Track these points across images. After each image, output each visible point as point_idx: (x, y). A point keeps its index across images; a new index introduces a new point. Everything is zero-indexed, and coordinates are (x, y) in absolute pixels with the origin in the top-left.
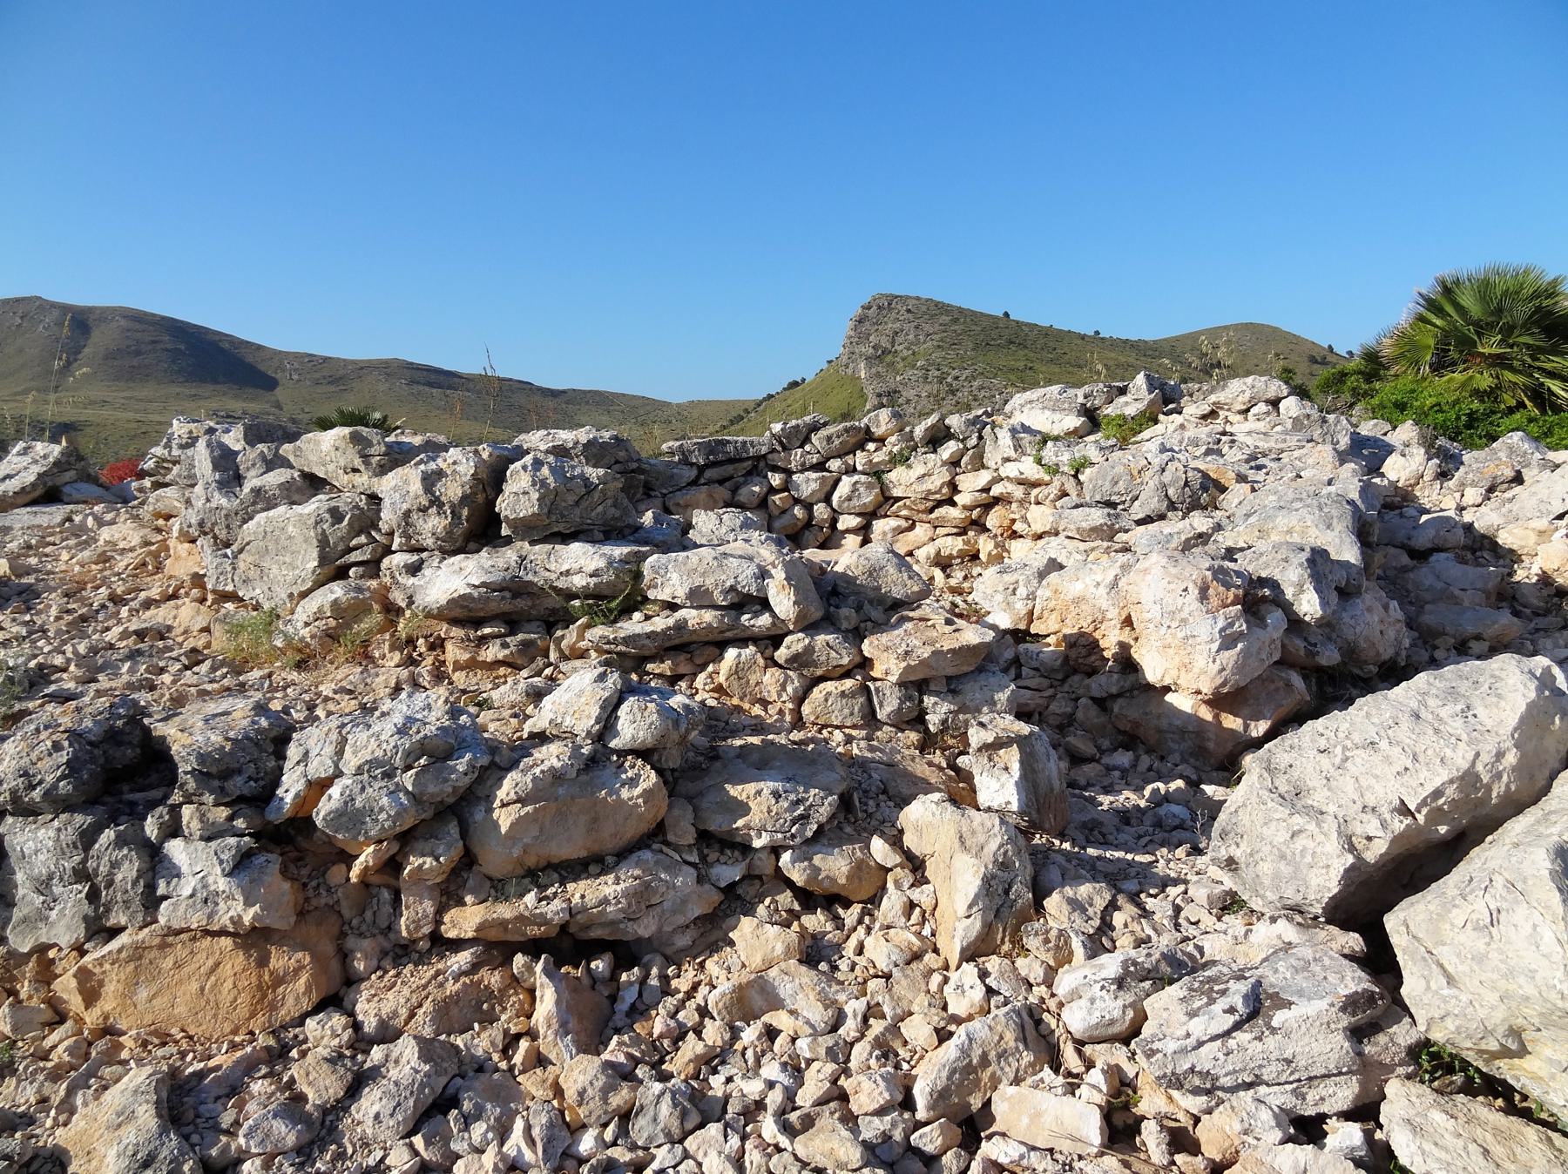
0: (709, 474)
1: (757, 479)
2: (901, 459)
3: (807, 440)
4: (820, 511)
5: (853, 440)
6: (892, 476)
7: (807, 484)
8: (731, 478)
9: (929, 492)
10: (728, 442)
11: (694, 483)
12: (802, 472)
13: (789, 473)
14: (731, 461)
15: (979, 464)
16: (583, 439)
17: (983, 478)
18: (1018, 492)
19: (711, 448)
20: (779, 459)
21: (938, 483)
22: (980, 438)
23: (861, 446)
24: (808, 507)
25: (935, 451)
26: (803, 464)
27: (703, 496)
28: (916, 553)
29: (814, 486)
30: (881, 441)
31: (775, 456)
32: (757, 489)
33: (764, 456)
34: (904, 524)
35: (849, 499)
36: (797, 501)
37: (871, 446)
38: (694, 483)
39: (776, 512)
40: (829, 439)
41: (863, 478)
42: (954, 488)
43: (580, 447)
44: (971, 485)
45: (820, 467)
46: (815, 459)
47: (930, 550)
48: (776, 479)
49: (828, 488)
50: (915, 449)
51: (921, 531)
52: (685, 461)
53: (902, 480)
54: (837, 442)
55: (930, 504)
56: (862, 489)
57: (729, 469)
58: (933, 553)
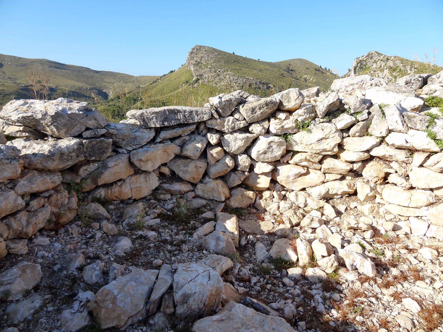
0: (164, 135)
1: (199, 138)
2: (302, 126)
3: (237, 110)
4: (243, 160)
5: (269, 111)
6: (296, 137)
7: (235, 142)
8: (180, 136)
9: (325, 150)
10: (179, 111)
12: (231, 133)
13: (222, 133)
14: (181, 125)
15: (365, 132)
16: (52, 111)
17: (368, 142)
18: (401, 155)
19: (166, 116)
20: (216, 124)
21: (332, 146)
22: (369, 113)
23: (273, 115)
24: (234, 157)
25: (330, 121)
26: (233, 128)
27: (160, 152)
28: (309, 190)
29: (240, 143)
30: (290, 112)
31: (213, 121)
32: (199, 145)
33: (205, 122)
34: (303, 171)
35: (265, 153)
36: (226, 153)
37: (282, 116)
38: (153, 141)
39: (212, 162)
40: (253, 110)
41: (276, 139)
42: (341, 146)
43: (48, 120)
44: (355, 147)
45: (245, 130)
46: (242, 124)
47: (322, 190)
48: (213, 139)
49: (249, 144)
50: (314, 119)
51: (315, 176)
52: (145, 126)
53: (301, 140)
54: (259, 113)
55: (320, 157)
56: (274, 146)
57: (179, 131)
58: (323, 192)
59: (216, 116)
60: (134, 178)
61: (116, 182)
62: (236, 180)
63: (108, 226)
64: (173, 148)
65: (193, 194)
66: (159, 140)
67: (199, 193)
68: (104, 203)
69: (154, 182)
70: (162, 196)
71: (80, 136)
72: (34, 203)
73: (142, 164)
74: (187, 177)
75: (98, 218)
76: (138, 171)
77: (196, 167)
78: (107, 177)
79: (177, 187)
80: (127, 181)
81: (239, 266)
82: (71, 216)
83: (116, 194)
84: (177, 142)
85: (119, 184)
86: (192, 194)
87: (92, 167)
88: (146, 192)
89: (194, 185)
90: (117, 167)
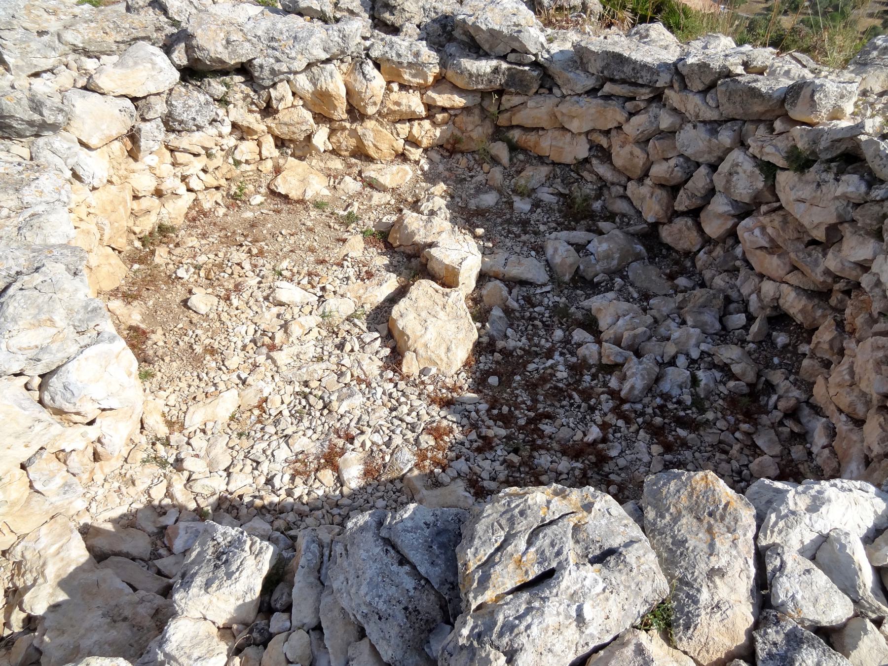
11: (592, 92)
21: (816, 222)
24: (698, 165)
27: (593, 111)
34: (764, 243)
41: (748, 166)
45: (713, 127)
46: (711, 115)
59: (676, 86)
60: (556, 133)
61: (536, 129)
62: (683, 202)
63: (497, 174)
64: (614, 115)
65: (621, 190)
66: (599, 94)
67: (629, 193)
68: (514, 148)
69: (582, 150)
70: (585, 174)
71: (504, 58)
72: (440, 117)
73: (566, 119)
74: (618, 161)
75: (495, 161)
76: (563, 128)
77: (632, 153)
78: (522, 117)
79: (603, 170)
80: (550, 133)
81: (548, 288)
82: (473, 146)
83: (531, 144)
84: (628, 105)
85: (541, 132)
86: (617, 190)
87: (516, 100)
88: (568, 159)
89: (629, 179)
90: (535, 110)
